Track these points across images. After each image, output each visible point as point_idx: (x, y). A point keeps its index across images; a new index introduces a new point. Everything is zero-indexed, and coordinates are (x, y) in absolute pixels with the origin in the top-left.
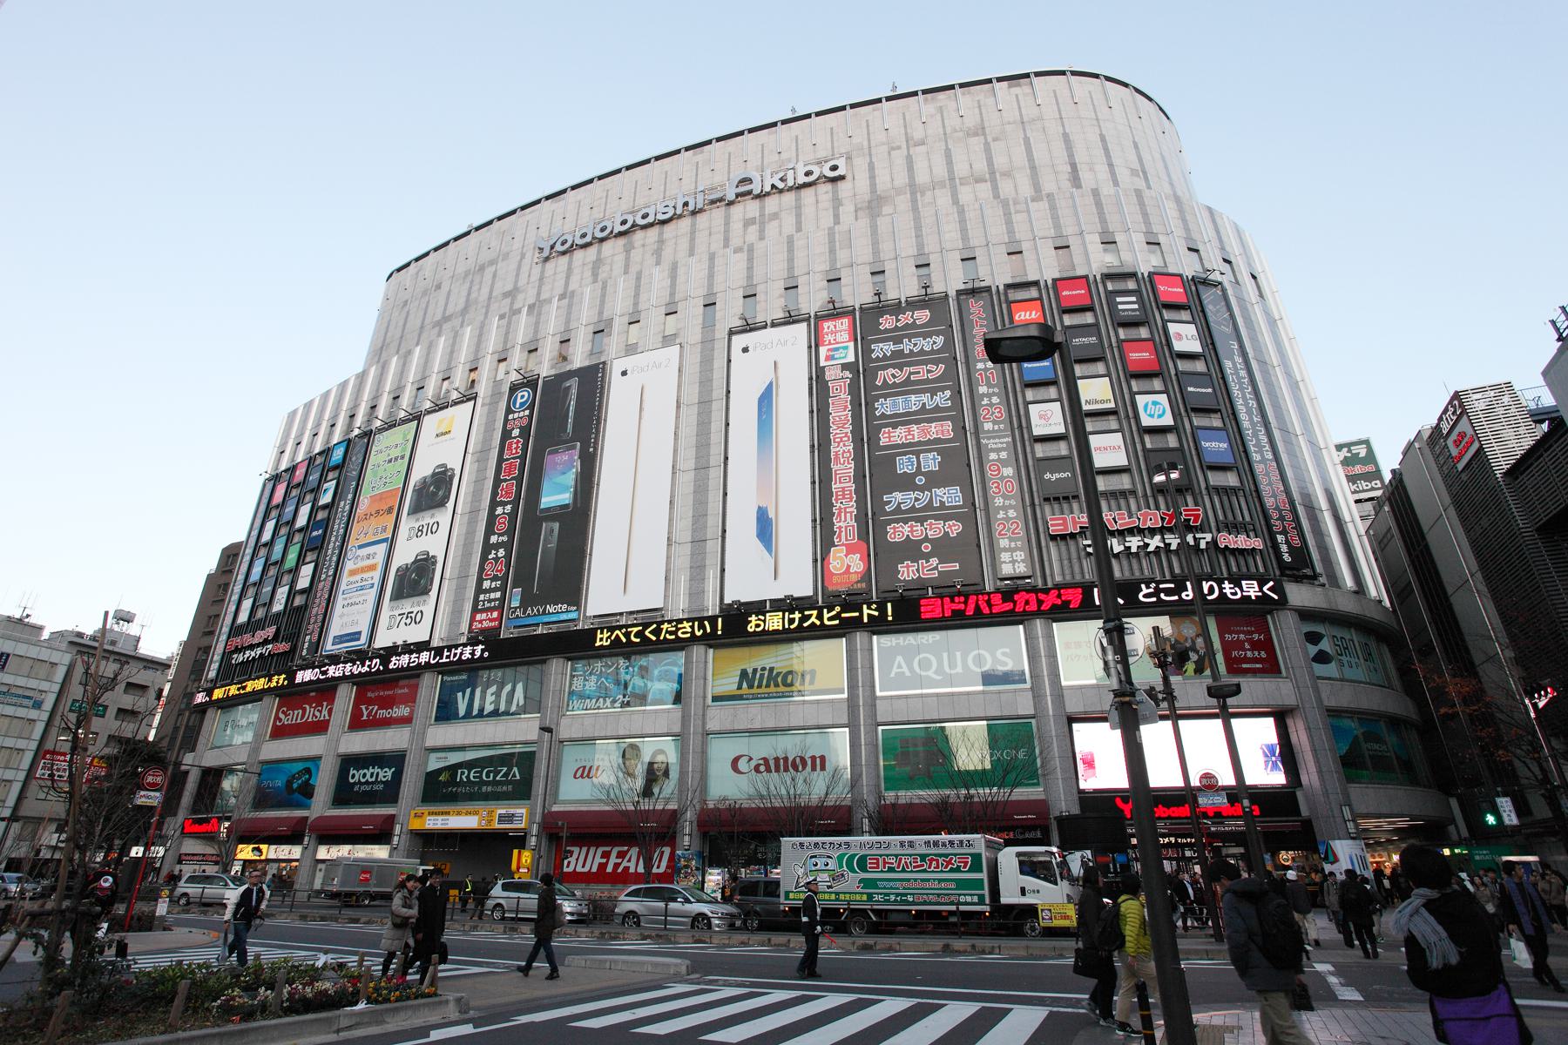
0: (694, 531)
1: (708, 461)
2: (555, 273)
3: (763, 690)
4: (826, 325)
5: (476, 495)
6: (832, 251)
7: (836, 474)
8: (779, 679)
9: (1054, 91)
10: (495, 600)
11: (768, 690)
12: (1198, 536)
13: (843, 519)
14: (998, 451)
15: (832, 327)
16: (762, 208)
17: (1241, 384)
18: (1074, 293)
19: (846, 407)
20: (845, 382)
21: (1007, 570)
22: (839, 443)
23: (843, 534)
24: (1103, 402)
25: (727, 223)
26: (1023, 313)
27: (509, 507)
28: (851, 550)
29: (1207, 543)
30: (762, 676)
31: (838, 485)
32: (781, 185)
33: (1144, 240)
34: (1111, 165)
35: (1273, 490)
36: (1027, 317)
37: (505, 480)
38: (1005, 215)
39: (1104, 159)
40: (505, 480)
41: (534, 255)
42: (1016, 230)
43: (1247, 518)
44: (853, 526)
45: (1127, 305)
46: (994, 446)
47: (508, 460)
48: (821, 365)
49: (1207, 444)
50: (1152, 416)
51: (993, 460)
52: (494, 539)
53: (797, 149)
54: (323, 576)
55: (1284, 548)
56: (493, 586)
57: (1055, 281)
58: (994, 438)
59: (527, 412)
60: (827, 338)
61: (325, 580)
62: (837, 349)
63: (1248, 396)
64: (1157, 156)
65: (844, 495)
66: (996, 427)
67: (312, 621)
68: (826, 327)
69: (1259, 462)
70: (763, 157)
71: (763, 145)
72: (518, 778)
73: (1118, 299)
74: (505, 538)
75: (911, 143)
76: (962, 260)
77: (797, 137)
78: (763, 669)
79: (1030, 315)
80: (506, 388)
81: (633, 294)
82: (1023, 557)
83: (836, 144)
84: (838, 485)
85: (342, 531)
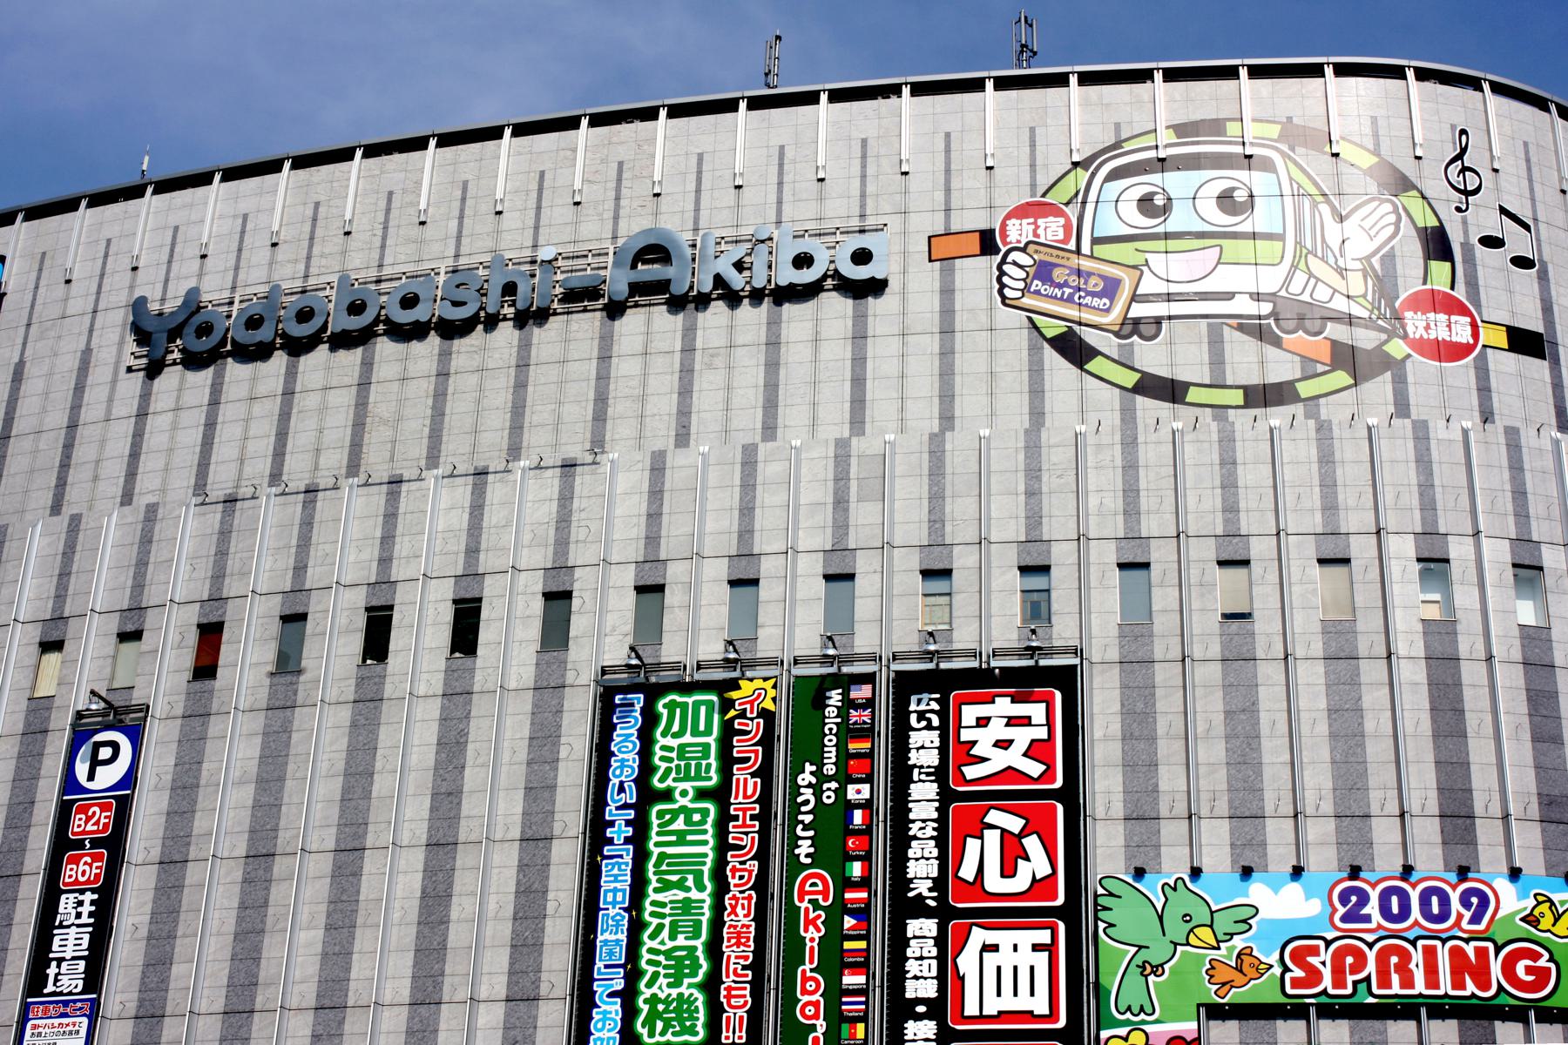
1: (536, 983)
2: (177, 409)
6: (841, 503)
16: (689, 332)
25: (605, 358)
32: (737, 281)
33: (1508, 559)
38: (1222, 463)
41: (121, 343)
42: (1242, 505)
53: (780, 184)
70: (698, 191)
71: (700, 157)
77: (782, 148)
80: (62, 723)
81: (378, 534)
83: (870, 189)
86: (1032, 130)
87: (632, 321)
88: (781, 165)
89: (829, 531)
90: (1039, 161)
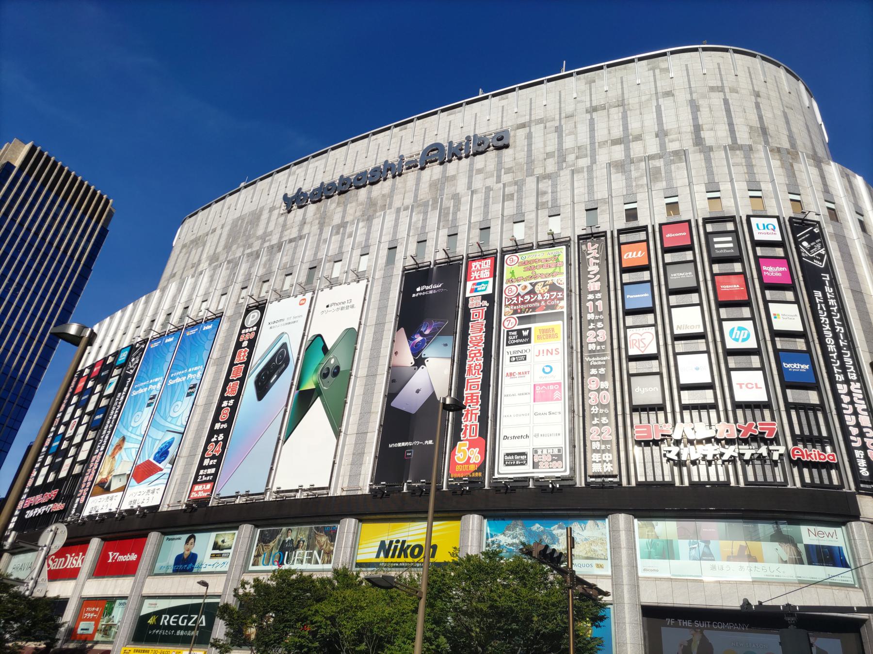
0: (359, 425)
3: (396, 560)
4: (474, 264)
5: (212, 390)
7: (468, 382)
8: (409, 551)
9: (686, 65)
10: (210, 475)
11: (399, 560)
12: (771, 448)
13: (469, 419)
14: (597, 367)
15: (478, 266)
17: (829, 311)
18: (677, 235)
19: (482, 329)
20: (483, 310)
21: (595, 468)
22: (473, 357)
23: (468, 431)
24: (693, 327)
26: (631, 253)
27: (232, 401)
28: (472, 444)
29: (781, 455)
30: (396, 547)
31: (469, 391)
33: (746, 188)
34: (731, 125)
35: (855, 409)
36: (634, 256)
37: (233, 380)
39: (726, 119)
40: (233, 380)
43: (824, 433)
44: (476, 425)
45: (724, 244)
46: (595, 363)
47: (237, 364)
48: (467, 296)
49: (789, 366)
50: (736, 340)
51: (593, 375)
52: (217, 426)
53: (475, 124)
54: (97, 451)
55: (862, 463)
56: (211, 464)
57: (661, 225)
58: (595, 356)
59: (255, 328)
60: (474, 275)
61: (97, 454)
62: (480, 284)
63: (836, 322)
64: (779, 113)
65: (472, 399)
66: (598, 348)
67: (83, 486)
68: (473, 266)
69: (842, 383)
70: (449, 131)
72: (204, 624)
73: (715, 240)
74: (225, 426)
75: (563, 115)
76: (587, 210)
78: (398, 541)
79: (636, 255)
82: (611, 459)
84: (469, 391)
85: (115, 416)
86: (560, 92)
87: (426, 173)
88: (476, 118)
89: (482, 215)
90: (562, 100)
